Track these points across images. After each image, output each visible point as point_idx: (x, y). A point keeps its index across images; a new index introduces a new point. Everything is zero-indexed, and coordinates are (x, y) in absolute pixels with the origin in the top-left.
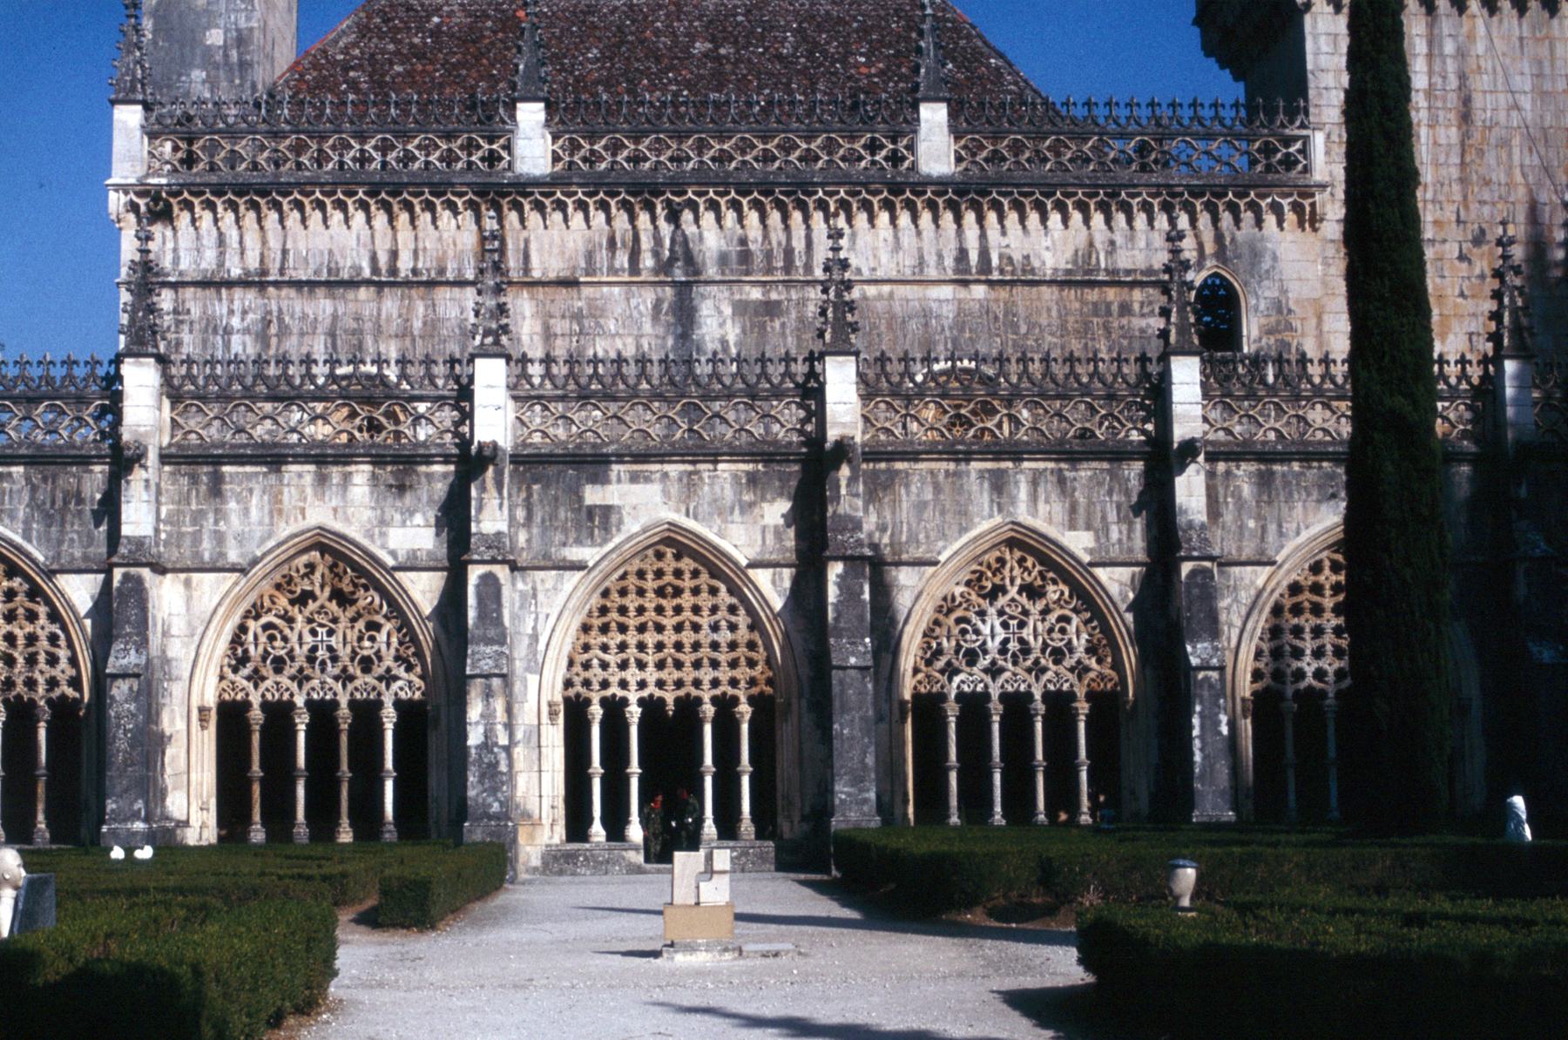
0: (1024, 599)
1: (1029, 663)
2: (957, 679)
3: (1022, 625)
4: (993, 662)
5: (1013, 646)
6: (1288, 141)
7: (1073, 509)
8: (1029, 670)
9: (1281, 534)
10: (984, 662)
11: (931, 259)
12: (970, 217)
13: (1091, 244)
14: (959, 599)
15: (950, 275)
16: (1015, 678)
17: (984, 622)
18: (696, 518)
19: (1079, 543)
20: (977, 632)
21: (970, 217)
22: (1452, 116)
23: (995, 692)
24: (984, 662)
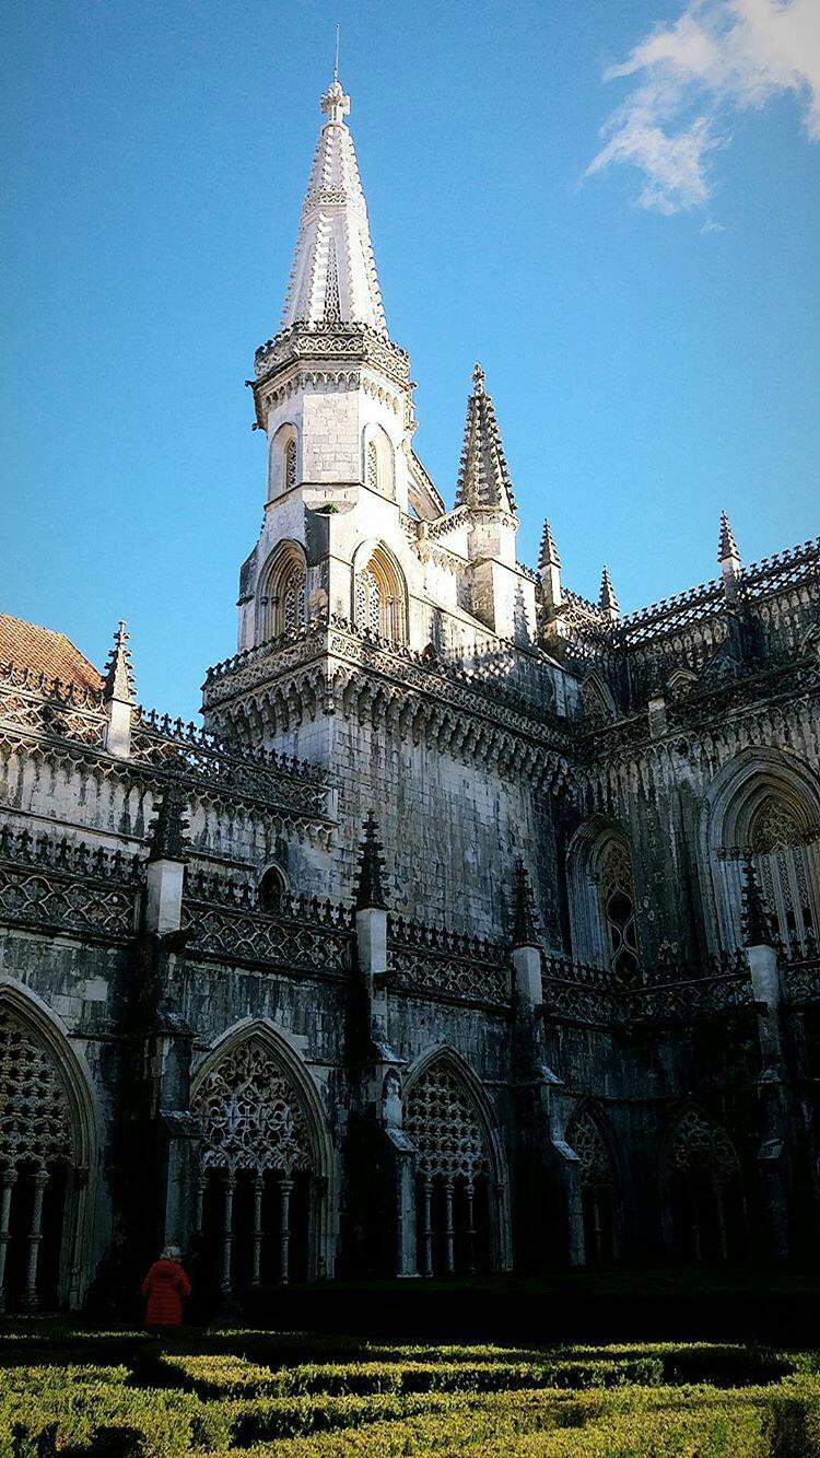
0: (255, 1089)
1: (255, 1143)
2: (209, 1154)
3: (253, 1110)
4: (232, 1142)
5: (246, 1128)
6: (318, 791)
7: (296, 1017)
8: (255, 1150)
9: (412, 1053)
10: (225, 1142)
11: (106, 817)
12: (135, 793)
13: (206, 830)
14: (214, 1085)
15: (117, 831)
16: (246, 1159)
17: (228, 1105)
18: (30, 986)
19: (298, 1043)
20: (223, 1114)
21: (135, 793)
22: (395, 798)
23: (233, 1170)
24: (225, 1142)
